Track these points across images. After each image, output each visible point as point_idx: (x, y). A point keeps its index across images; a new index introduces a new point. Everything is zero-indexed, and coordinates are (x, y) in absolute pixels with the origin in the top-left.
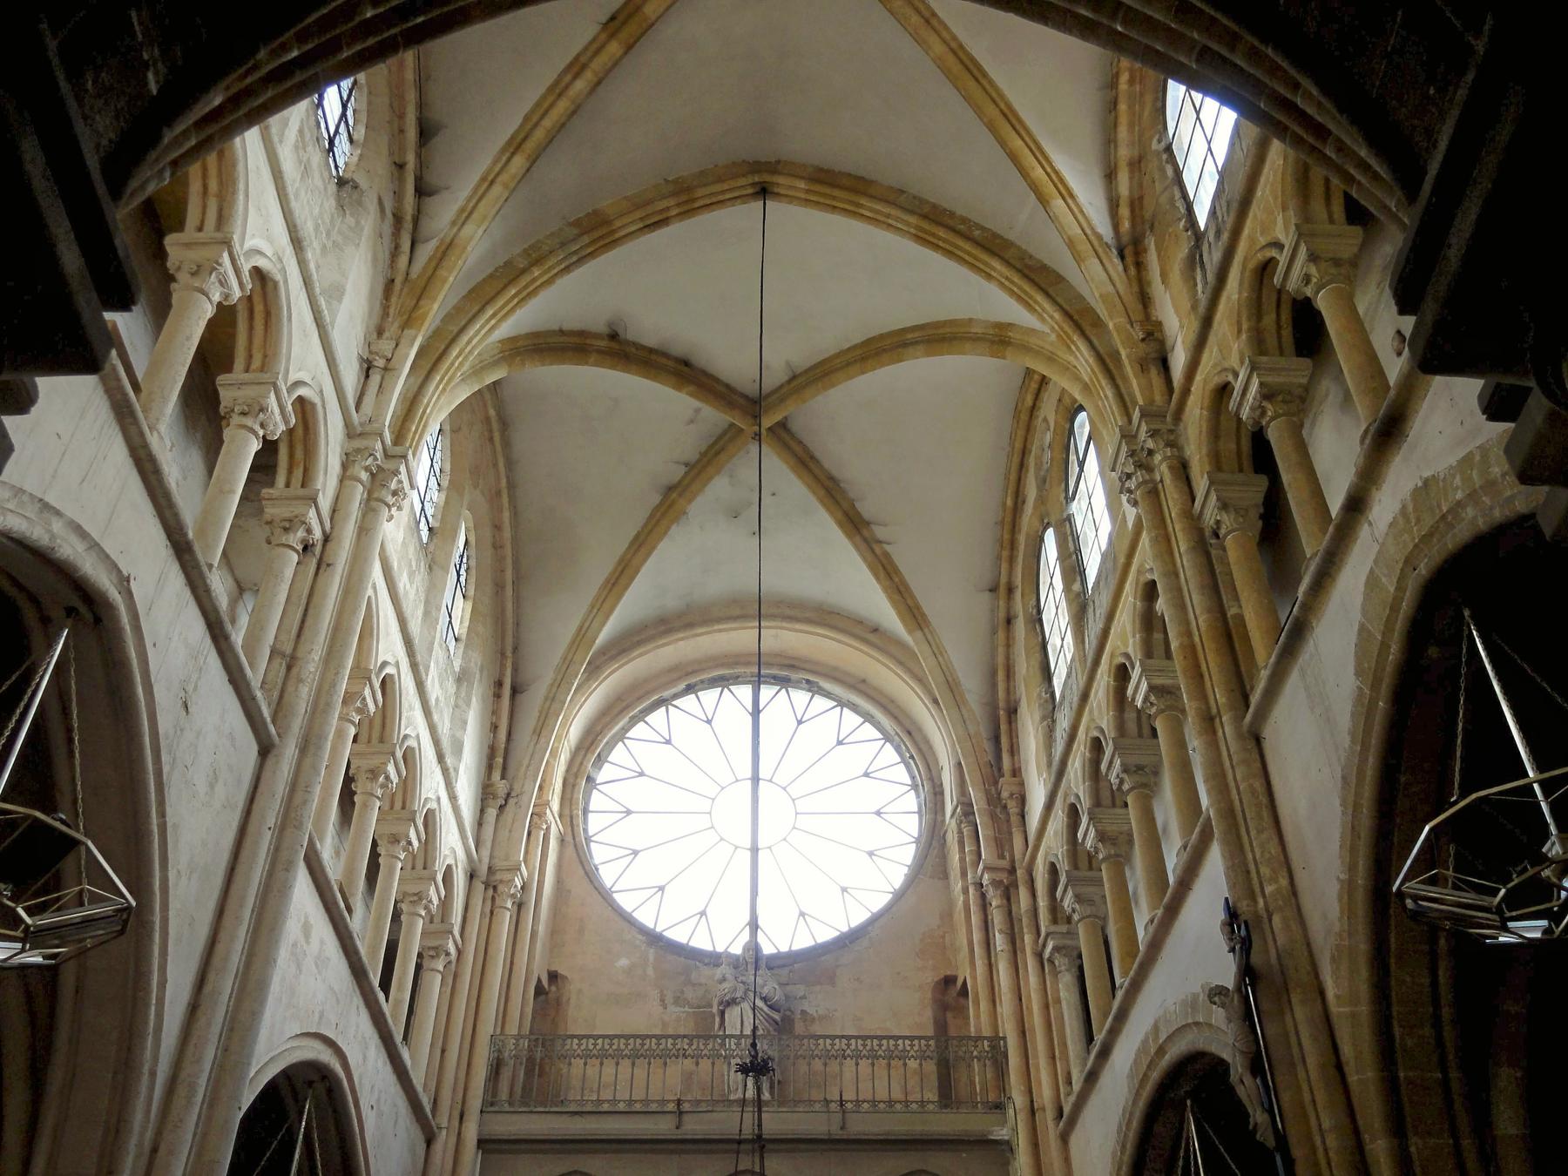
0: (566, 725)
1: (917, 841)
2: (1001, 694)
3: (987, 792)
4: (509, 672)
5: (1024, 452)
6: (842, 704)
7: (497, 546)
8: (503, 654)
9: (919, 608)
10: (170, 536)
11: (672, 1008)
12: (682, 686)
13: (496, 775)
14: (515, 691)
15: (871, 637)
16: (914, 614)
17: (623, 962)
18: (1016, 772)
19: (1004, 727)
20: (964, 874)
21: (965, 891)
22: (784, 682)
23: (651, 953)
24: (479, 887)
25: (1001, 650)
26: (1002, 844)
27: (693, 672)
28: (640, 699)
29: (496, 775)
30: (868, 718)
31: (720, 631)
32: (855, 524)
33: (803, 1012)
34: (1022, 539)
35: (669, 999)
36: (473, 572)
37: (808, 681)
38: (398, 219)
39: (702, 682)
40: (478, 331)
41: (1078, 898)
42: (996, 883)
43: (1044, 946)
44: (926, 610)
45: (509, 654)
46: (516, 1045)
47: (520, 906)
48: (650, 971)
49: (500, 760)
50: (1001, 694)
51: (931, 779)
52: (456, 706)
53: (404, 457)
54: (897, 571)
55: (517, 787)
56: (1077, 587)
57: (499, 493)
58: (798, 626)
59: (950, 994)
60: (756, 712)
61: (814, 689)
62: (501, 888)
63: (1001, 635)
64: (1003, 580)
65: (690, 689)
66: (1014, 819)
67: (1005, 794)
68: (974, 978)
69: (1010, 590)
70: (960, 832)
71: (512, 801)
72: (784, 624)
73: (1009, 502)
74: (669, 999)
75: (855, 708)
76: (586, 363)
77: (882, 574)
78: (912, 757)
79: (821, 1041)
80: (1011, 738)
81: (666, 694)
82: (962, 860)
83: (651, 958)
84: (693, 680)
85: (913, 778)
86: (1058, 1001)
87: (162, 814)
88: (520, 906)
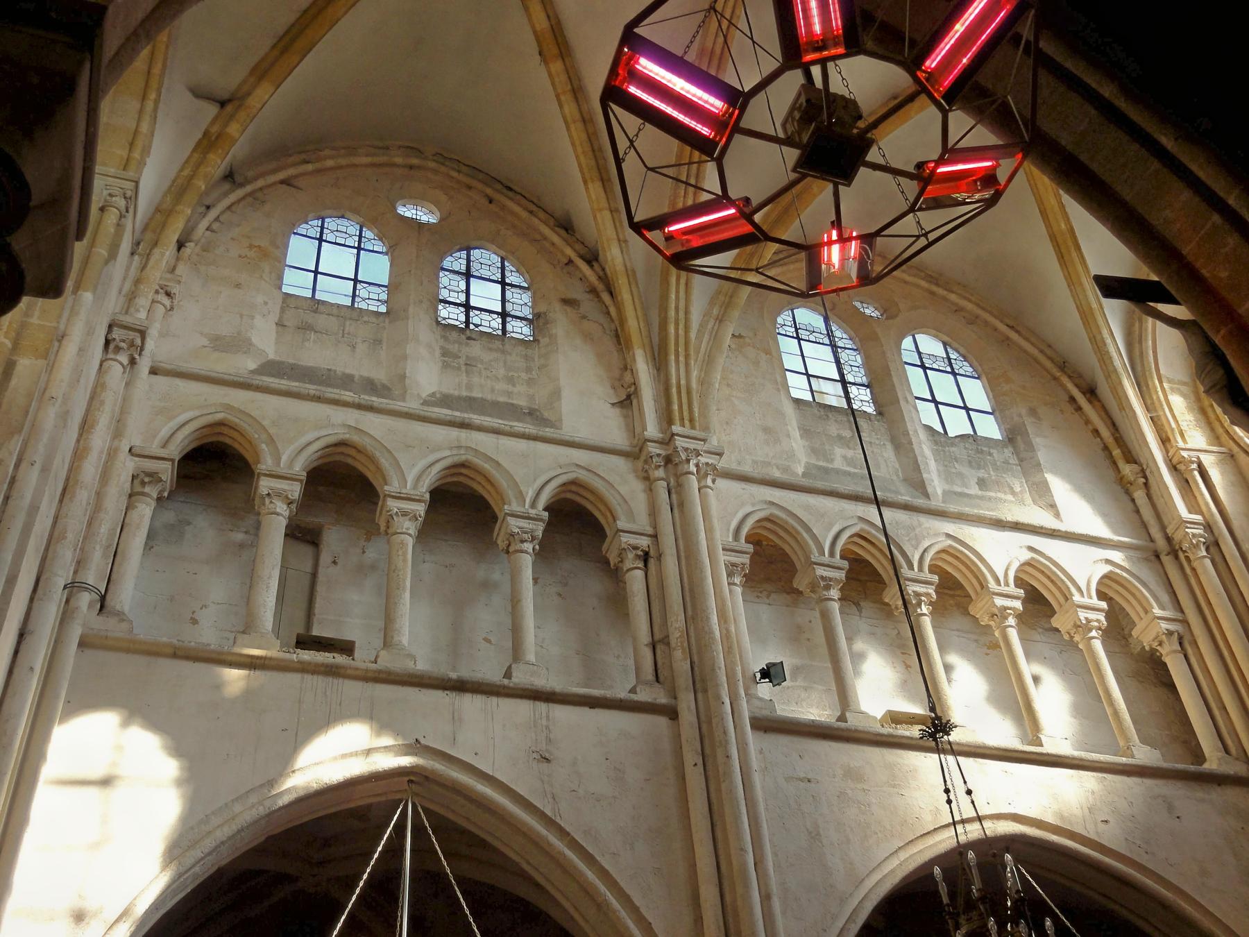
4: (1070, 386)
7: (973, 320)
8: (1055, 379)
10: (444, 688)
24: (1167, 560)
29: (1122, 464)
36: (970, 356)
38: (593, 291)
40: (677, 298)
47: (1214, 545)
49: (1117, 452)
52: (1021, 460)
53: (673, 435)
55: (1142, 460)
57: (932, 293)
62: (1185, 546)
71: (1148, 473)
76: (815, 196)
87: (563, 833)
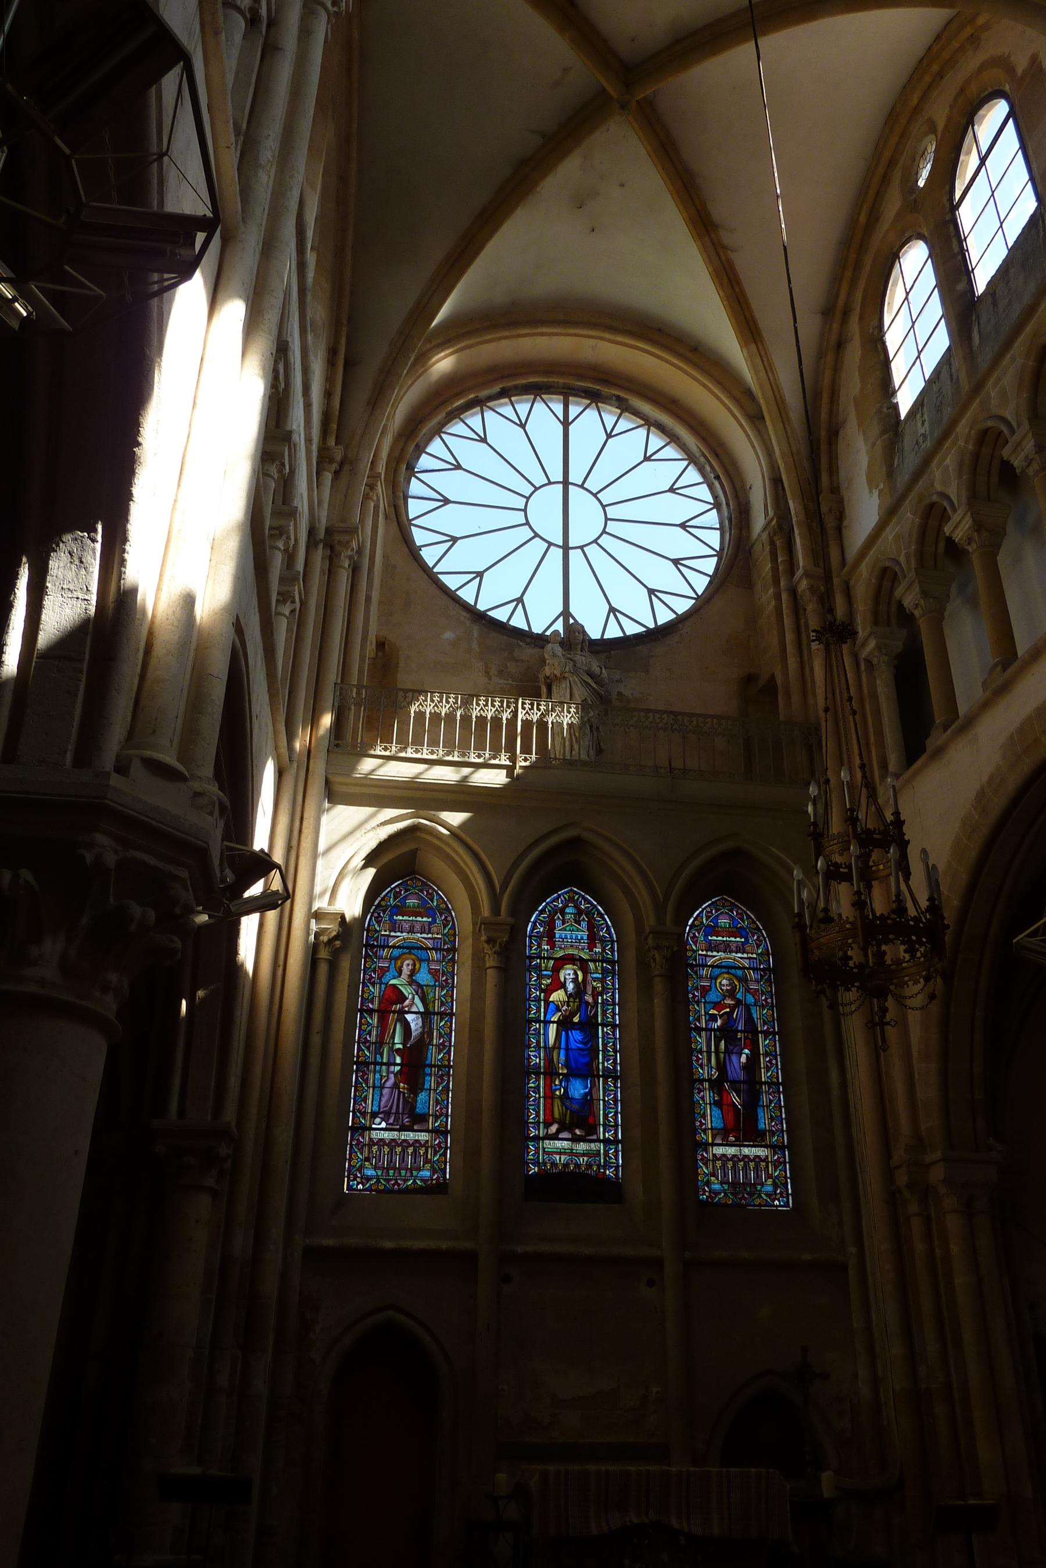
0: (395, 406)
1: (719, 555)
2: (824, 416)
3: (806, 508)
5: (892, 163)
6: (649, 423)
9: (755, 322)
11: (496, 680)
12: (496, 389)
13: (332, 442)
14: (348, 364)
15: (690, 355)
16: (749, 329)
17: (448, 635)
18: (835, 490)
19: (824, 448)
20: (776, 581)
21: (778, 597)
22: (595, 398)
23: (476, 630)
25: (828, 373)
26: (819, 553)
27: (510, 376)
28: (458, 395)
30: (673, 439)
31: (542, 334)
32: (704, 225)
33: (619, 694)
34: (868, 260)
35: (493, 671)
37: (618, 398)
39: (516, 387)
41: (924, 593)
42: (812, 589)
43: (863, 645)
44: (762, 324)
45: (345, 322)
46: (358, 693)
48: (475, 645)
49: (334, 426)
50: (824, 416)
51: (736, 496)
54: (738, 282)
56: (961, 287)
58: (620, 338)
59: (757, 690)
60: (566, 423)
61: (624, 408)
63: (830, 357)
64: (841, 302)
65: (505, 393)
66: (831, 532)
67: (824, 509)
68: (785, 673)
69: (846, 313)
70: (772, 543)
71: (346, 468)
72: (607, 335)
73: (863, 219)
74: (493, 671)
75: (662, 429)
77: (726, 281)
78: (717, 478)
79: (651, 715)
80: (830, 459)
81: (484, 393)
82: (775, 569)
83: (476, 633)
84: (510, 384)
85: (715, 497)
86: (874, 696)
88: (355, 569)
